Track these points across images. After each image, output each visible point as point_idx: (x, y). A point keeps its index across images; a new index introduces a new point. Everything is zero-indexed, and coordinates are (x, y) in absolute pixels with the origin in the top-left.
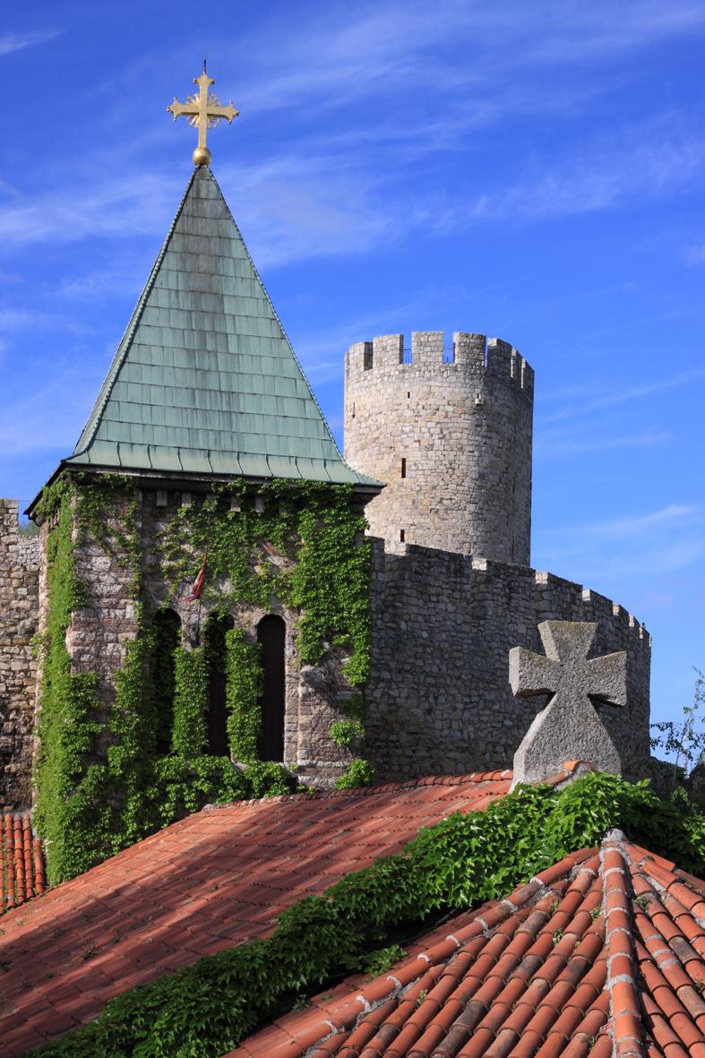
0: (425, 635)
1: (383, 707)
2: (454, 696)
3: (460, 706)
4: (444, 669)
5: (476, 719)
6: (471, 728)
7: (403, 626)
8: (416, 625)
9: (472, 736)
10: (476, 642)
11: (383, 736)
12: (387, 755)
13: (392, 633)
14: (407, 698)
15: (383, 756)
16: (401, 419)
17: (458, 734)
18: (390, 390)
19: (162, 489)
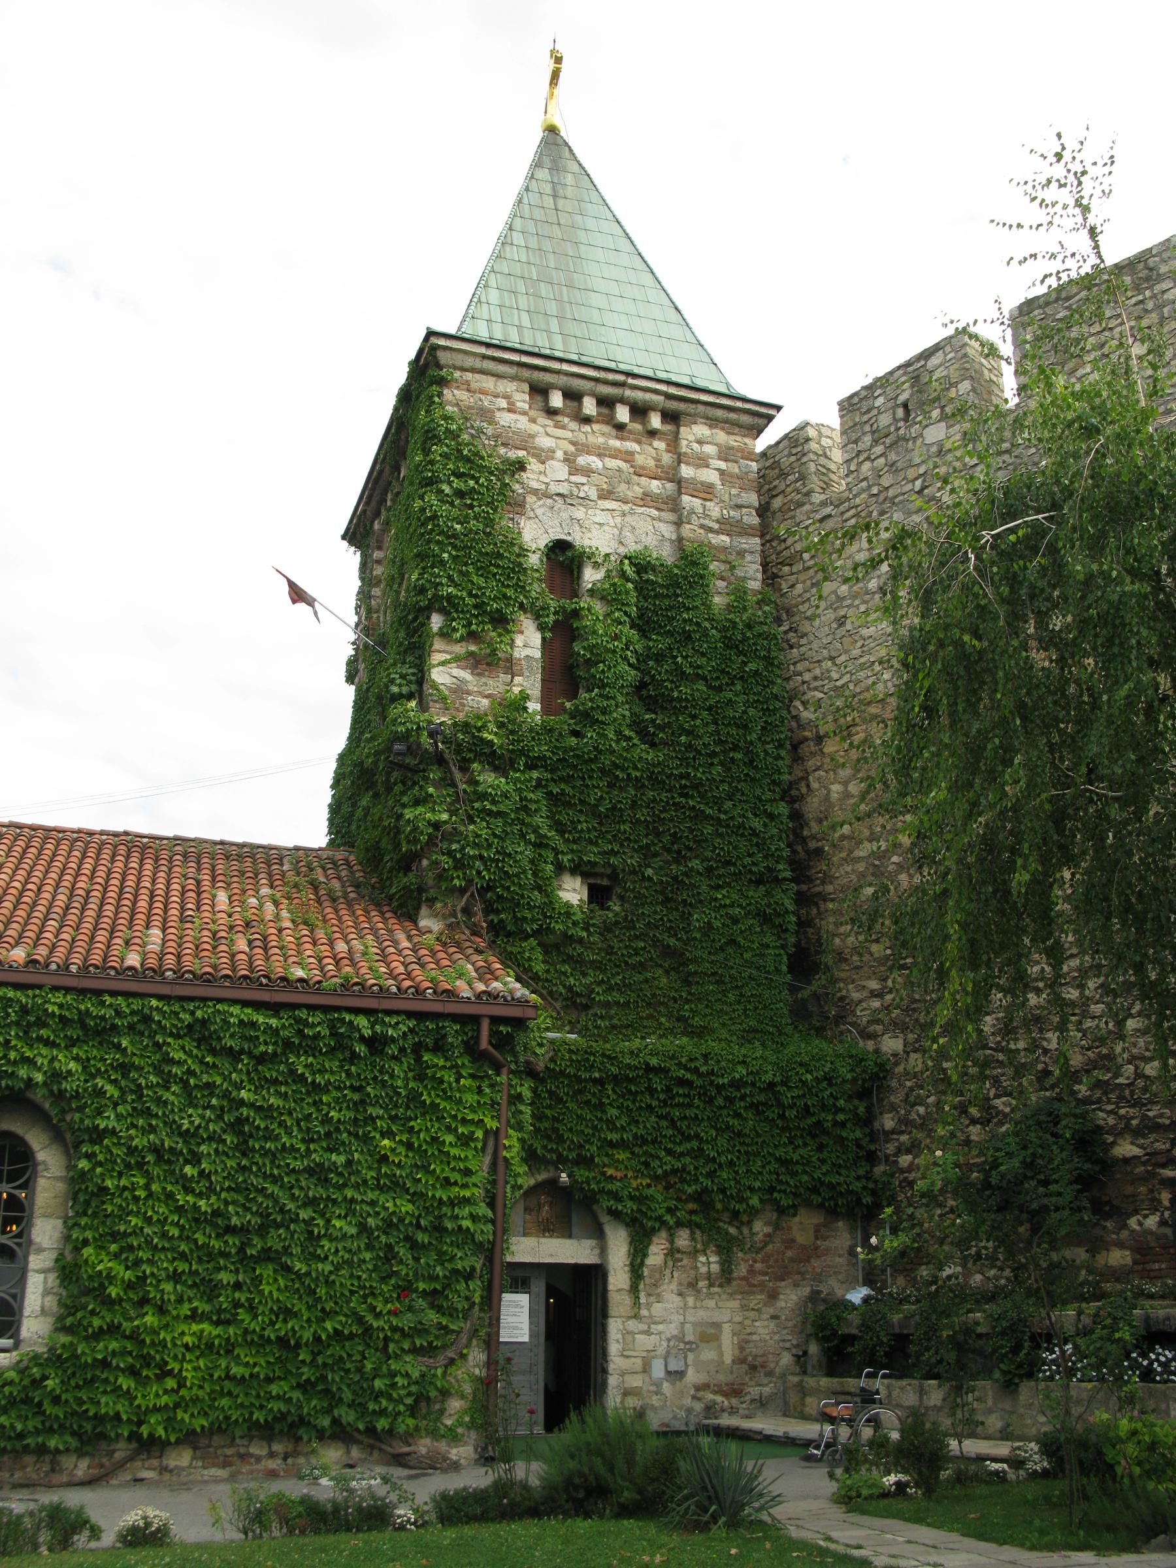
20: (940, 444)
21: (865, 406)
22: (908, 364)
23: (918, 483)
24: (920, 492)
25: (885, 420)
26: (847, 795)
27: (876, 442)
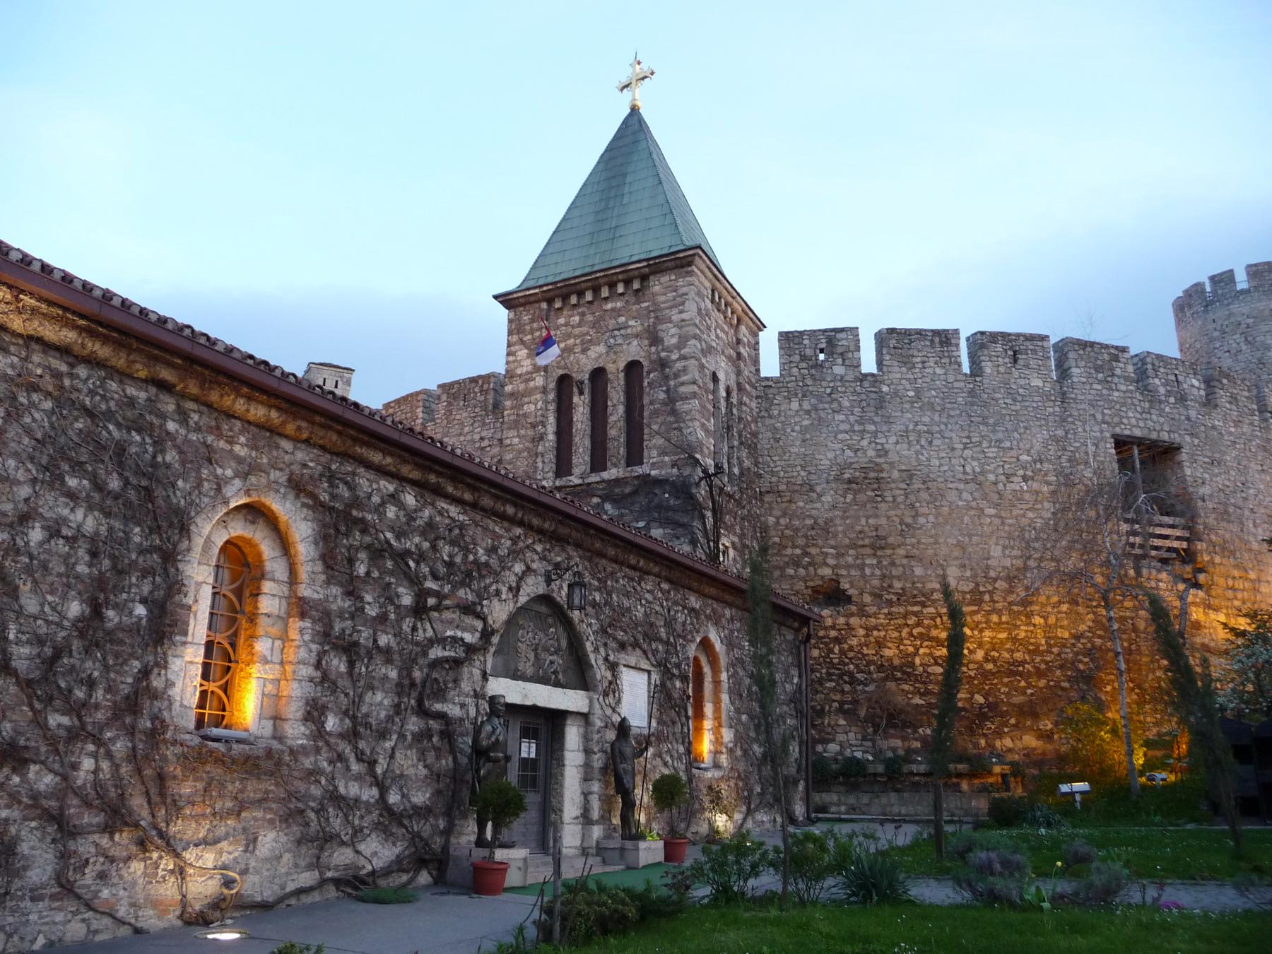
0: (911, 394)
1: (871, 453)
2: (951, 438)
3: (961, 446)
4: (936, 417)
5: (981, 456)
6: (975, 463)
7: (885, 389)
9: (978, 470)
10: (972, 393)
11: (872, 475)
12: (879, 489)
13: (873, 396)
14: (897, 443)
15: (874, 490)
16: (1212, 340)
18: (1200, 323)
19: (558, 296)
20: (842, 377)
21: (796, 340)
22: (825, 331)
23: (828, 391)
24: (830, 395)
25: (809, 352)
26: (778, 523)
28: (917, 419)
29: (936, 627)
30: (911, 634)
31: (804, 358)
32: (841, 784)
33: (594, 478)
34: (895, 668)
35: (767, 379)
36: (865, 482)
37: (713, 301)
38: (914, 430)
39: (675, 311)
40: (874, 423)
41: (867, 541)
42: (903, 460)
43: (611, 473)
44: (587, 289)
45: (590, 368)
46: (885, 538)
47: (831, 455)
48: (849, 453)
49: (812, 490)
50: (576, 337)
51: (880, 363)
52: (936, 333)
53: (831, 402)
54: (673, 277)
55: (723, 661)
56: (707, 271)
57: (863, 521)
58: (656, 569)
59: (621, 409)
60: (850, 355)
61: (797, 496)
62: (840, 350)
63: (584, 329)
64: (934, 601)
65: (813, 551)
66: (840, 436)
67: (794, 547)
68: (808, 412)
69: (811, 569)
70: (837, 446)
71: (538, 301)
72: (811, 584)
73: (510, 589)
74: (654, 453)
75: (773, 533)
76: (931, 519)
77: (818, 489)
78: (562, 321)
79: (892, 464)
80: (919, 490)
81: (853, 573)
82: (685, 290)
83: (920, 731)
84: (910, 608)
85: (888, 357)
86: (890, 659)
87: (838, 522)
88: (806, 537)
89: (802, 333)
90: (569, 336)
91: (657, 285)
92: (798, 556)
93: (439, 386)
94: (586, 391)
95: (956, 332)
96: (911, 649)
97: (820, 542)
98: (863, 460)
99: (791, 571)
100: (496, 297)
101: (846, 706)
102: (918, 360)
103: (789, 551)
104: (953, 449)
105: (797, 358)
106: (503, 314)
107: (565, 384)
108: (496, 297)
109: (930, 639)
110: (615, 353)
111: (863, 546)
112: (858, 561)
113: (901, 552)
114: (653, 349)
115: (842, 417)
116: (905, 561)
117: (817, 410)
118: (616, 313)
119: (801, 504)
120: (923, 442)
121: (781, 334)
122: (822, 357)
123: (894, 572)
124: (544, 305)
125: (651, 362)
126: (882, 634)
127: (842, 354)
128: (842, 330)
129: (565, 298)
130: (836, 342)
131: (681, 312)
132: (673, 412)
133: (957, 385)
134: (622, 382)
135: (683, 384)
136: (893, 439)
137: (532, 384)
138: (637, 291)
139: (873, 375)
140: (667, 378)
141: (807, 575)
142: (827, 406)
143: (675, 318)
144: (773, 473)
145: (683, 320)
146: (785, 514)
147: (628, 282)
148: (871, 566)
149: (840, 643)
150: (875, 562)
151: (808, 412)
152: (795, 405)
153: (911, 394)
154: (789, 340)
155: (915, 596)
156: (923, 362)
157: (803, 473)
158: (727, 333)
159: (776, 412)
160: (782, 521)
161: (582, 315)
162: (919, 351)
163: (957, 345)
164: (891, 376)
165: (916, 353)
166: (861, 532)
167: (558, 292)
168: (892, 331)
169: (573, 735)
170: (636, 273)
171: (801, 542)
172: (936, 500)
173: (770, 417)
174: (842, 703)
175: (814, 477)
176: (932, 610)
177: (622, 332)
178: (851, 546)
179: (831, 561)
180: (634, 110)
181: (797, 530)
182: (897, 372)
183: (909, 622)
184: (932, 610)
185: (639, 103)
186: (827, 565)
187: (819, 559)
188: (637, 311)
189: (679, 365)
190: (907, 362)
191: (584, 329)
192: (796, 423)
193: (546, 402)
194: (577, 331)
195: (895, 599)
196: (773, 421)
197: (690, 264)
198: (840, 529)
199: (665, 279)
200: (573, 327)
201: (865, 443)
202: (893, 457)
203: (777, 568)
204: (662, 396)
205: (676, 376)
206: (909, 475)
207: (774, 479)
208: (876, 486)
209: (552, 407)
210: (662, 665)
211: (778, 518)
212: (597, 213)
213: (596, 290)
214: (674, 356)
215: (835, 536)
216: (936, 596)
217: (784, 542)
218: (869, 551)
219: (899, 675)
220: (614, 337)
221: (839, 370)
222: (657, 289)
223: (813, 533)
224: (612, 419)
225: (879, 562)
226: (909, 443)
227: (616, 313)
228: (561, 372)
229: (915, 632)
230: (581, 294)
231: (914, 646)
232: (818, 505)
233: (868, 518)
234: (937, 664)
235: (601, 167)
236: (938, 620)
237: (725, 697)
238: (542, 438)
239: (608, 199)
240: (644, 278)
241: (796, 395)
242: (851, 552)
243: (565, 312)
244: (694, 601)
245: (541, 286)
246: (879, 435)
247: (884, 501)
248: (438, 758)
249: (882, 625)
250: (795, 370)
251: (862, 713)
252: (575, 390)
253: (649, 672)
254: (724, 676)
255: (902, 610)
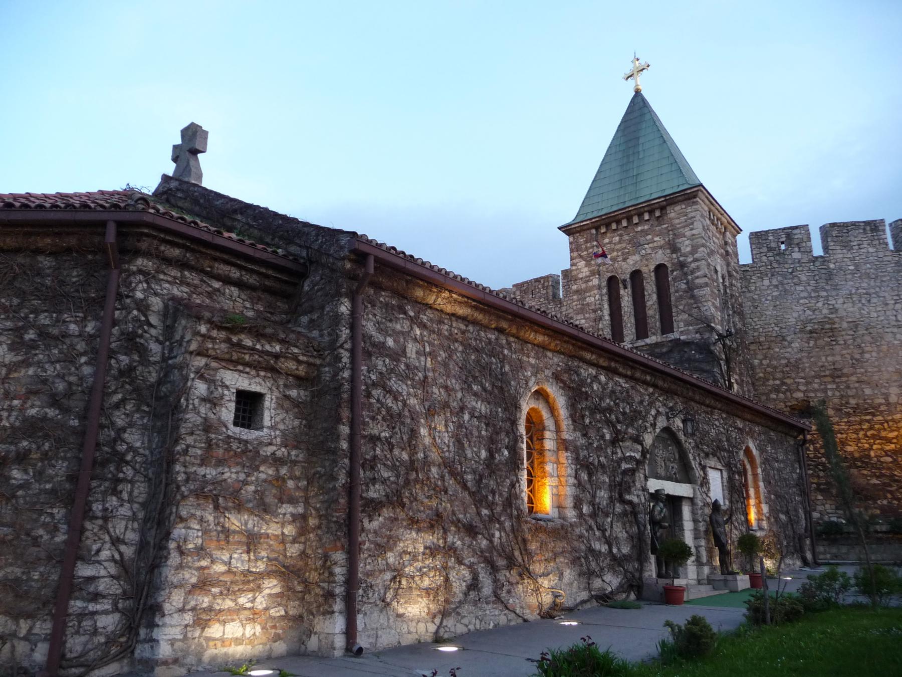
1: (825, 311)
2: (884, 297)
3: (893, 302)
7: (832, 266)
8: (843, 264)
11: (828, 326)
12: (833, 336)
13: (823, 271)
14: (844, 303)
15: (829, 337)
17: (894, 318)
21: (764, 237)
22: (784, 229)
23: (790, 270)
24: (791, 273)
25: (773, 245)
26: (761, 364)
27: (769, 251)
28: (857, 285)
29: (885, 429)
30: (866, 435)
31: (770, 249)
32: (824, 540)
33: (640, 343)
34: (856, 459)
35: (744, 266)
36: (823, 332)
37: (710, 219)
38: (856, 293)
39: (687, 229)
40: (826, 290)
41: (827, 373)
42: (850, 315)
43: (652, 339)
44: (623, 218)
45: (630, 270)
46: (840, 370)
47: (795, 315)
48: (808, 312)
49: (784, 339)
50: (618, 251)
51: (826, 248)
52: (867, 223)
53: (793, 279)
54: (684, 206)
55: (758, 460)
56: (706, 200)
57: (823, 359)
58: (719, 406)
59: (655, 297)
60: (804, 244)
61: (773, 344)
62: (796, 241)
63: (623, 245)
64: (882, 412)
65: (789, 381)
66: (802, 301)
67: (776, 379)
68: (776, 286)
69: (788, 394)
70: (800, 308)
71: (590, 229)
72: (789, 404)
73: (651, 425)
74: (682, 324)
75: (758, 371)
76: (874, 354)
77: (789, 339)
78: (607, 240)
79: (841, 318)
80: (863, 335)
81: (819, 395)
82: (693, 214)
83: (879, 502)
84: (863, 417)
85: (832, 244)
86: (851, 453)
87: (805, 360)
88: (783, 372)
89: (767, 232)
90: (613, 250)
91: (673, 213)
92: (777, 385)
93: (514, 286)
94: (629, 286)
95: (882, 221)
96: (867, 446)
97: (793, 375)
98: (819, 317)
99: (773, 396)
100: (560, 228)
101: (822, 487)
102: (855, 243)
103: (771, 382)
104: (887, 304)
105: (765, 249)
106: (565, 239)
107: (612, 282)
108: (560, 228)
109: (881, 438)
110: (647, 260)
111: (825, 376)
112: (822, 387)
113: (854, 378)
114: (674, 256)
115: (801, 288)
116: (857, 385)
117: (782, 284)
118: (645, 233)
119: (777, 350)
120: (863, 301)
121: (751, 234)
122: (783, 247)
123: (850, 393)
124: (594, 231)
125: (673, 264)
126: (844, 436)
127: (798, 244)
128: (796, 227)
129: (608, 225)
130: (792, 236)
131: (692, 229)
132: (693, 297)
133: (886, 259)
134: (654, 279)
135: (697, 277)
136: (841, 301)
137: (590, 284)
138: (659, 217)
139: (821, 257)
140: (686, 274)
141: (786, 398)
142: (790, 281)
143: (688, 234)
144: (754, 330)
145: (693, 235)
146: (765, 358)
147: (651, 212)
148: (832, 389)
149: (813, 444)
150: (834, 386)
151: (776, 286)
152: (766, 282)
153: (852, 268)
154: (757, 238)
155: (866, 409)
156: (859, 245)
157: (776, 329)
158: (718, 239)
159: (753, 288)
160: (764, 362)
161: (621, 235)
162: (856, 237)
163: (884, 231)
164: (836, 257)
165: (852, 239)
166: (822, 366)
167: (602, 222)
168: (833, 225)
169: (686, 510)
170: (657, 205)
171: (779, 375)
172: (877, 341)
173: (749, 291)
174: (818, 484)
175: (785, 331)
176: (880, 418)
177: (651, 245)
178: (815, 377)
179: (802, 388)
180: (638, 93)
181: (775, 368)
182: (839, 253)
183: (864, 427)
184: (880, 418)
185: (640, 87)
186: (800, 390)
187: (794, 387)
188: (660, 231)
189: (693, 265)
190: (847, 246)
191: (623, 245)
192: (768, 295)
193: (601, 295)
194: (618, 247)
195: (851, 411)
196: (751, 294)
197: (695, 197)
198: (807, 365)
199: (677, 208)
200: (615, 244)
201: (820, 305)
202: (841, 313)
203: (763, 394)
204: (684, 286)
205: (692, 272)
206: (855, 325)
207: (756, 334)
208: (831, 334)
209: (606, 298)
210: (728, 466)
211: (761, 360)
212: (622, 166)
213: (629, 219)
214: (690, 259)
215: (804, 370)
216: (883, 408)
217: (767, 376)
218: (829, 379)
219: (859, 464)
220: (645, 249)
221: (796, 255)
222: (672, 215)
223: (788, 369)
224: (649, 304)
225: (838, 387)
226: (853, 302)
227: (645, 233)
228: (610, 275)
229: (869, 433)
230: (618, 222)
231: (868, 443)
232: (789, 350)
233: (827, 356)
234: (887, 455)
235: (620, 134)
236: (886, 425)
237: (761, 484)
238: (601, 319)
239: (628, 156)
240: (663, 208)
241: (767, 275)
242: (817, 381)
243: (608, 235)
244: (740, 424)
245: (591, 219)
246: (830, 298)
247: (837, 344)
248: (631, 527)
249: (843, 429)
250: (764, 259)
251: (834, 491)
252: (621, 286)
253: (721, 470)
254: (759, 471)
255: (857, 419)
